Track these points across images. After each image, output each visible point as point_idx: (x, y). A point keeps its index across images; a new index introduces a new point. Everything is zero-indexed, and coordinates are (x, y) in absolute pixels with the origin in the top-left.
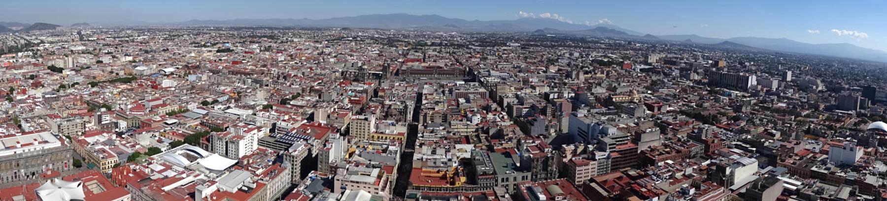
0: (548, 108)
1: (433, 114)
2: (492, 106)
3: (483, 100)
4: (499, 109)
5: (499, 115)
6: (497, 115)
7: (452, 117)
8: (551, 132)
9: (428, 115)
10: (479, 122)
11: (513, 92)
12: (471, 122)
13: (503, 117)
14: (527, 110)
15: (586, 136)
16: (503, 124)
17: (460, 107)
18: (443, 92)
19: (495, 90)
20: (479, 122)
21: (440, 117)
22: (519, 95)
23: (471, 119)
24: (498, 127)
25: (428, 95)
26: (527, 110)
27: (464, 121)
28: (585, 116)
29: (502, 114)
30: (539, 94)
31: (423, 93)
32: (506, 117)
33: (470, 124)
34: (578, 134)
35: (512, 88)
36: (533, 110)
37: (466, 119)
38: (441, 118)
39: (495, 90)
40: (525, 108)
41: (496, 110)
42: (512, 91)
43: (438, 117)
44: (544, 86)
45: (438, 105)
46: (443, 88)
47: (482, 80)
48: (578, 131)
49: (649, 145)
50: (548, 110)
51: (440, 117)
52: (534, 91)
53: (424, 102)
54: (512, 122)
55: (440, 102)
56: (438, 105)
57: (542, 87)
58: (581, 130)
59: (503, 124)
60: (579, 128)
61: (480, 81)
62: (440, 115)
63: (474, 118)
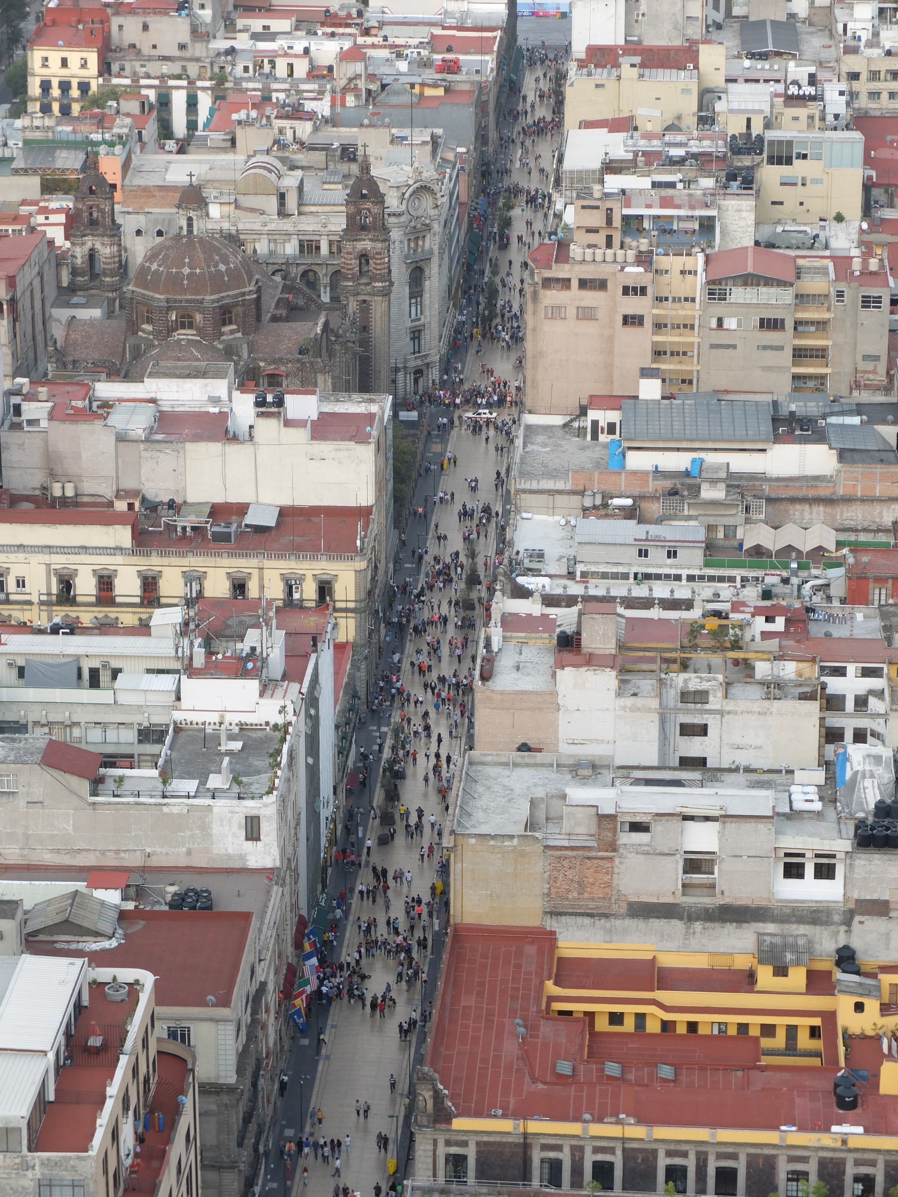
21: (770, 324)
51: (770, 324)
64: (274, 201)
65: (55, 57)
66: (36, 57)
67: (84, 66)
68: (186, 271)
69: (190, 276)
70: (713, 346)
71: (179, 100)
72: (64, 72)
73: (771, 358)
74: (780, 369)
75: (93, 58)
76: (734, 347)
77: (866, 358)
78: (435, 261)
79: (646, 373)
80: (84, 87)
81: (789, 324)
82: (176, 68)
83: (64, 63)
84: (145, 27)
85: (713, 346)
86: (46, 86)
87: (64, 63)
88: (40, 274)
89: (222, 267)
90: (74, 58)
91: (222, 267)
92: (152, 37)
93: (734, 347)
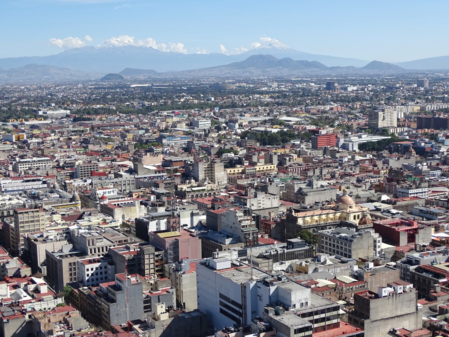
0: (146, 257)
2: (7, 266)
4: (26, 271)
5: (26, 285)
6: (22, 285)
8: (159, 313)
11: (60, 227)
13: (37, 290)
14: (97, 265)
15: (240, 315)
16: (37, 306)
19: (13, 225)
22: (73, 231)
24: (27, 317)
26: (97, 265)
28: (233, 265)
29: (34, 282)
30: (124, 225)
32: (44, 289)
34: (222, 311)
35: (57, 218)
36: (111, 263)
39: (13, 225)
40: (90, 262)
41: (17, 275)
42: (57, 224)
44: (133, 205)
48: (221, 303)
49: (389, 328)
50: (147, 262)
52: (111, 218)
54: (60, 301)
57: (128, 209)
58: (227, 299)
59: (37, 306)
60: (221, 296)
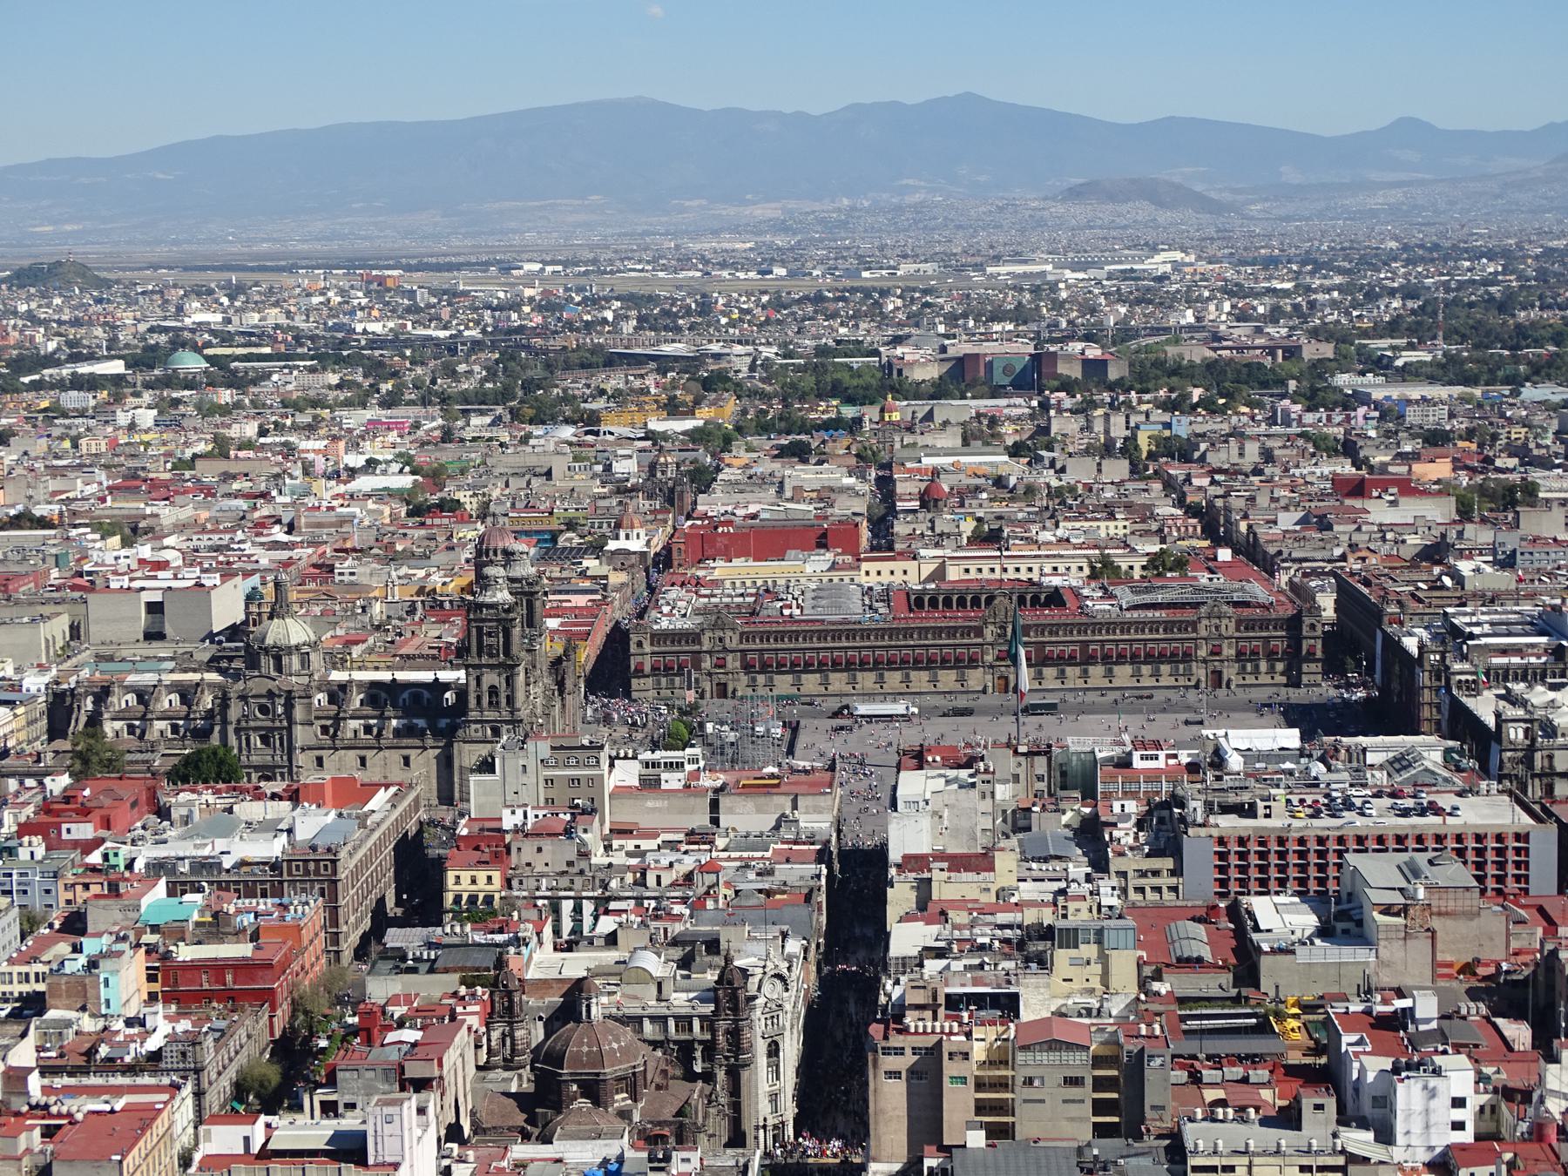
1: (999, 1059)
3: (1493, 919)
7: (1196, 1079)
9: (950, 1068)
10: (1467, 1136)
12: (1385, 1136)
17: (1266, 984)
18: (1091, 835)
20: (1467, 1136)
23: (1385, 1102)
25: (937, 875)
27: (1318, 1126)
31: (895, 855)
33: (1376, 1152)
37: (1331, 1104)
38: (1087, 1093)
43: (1052, 1090)
45: (1043, 963)
46: (1089, 794)
47: (1484, 707)
53: (906, 938)
55: (1070, 938)
56: (1043, 963)
61: (1461, 724)
62: (1077, 1063)
63: (1408, 1094)
64: (654, 989)
65: (466, 876)
66: (450, 876)
67: (489, 878)
68: (585, 1049)
69: (589, 1053)
70: (1025, 1101)
71: (567, 907)
72: (473, 887)
73: (1074, 1109)
74: (1081, 1119)
75: (497, 876)
76: (1042, 1101)
77: (1153, 1107)
78: (787, 1033)
79: (970, 1126)
80: (489, 900)
81: (1089, 1082)
82: (564, 882)
83: (474, 881)
84: (540, 850)
85: (1025, 1101)
86: (457, 899)
87: (474, 881)
88: (462, 1055)
89: (615, 1046)
90: (482, 876)
91: (615, 1046)
92: (547, 855)
93: (1042, 1101)
